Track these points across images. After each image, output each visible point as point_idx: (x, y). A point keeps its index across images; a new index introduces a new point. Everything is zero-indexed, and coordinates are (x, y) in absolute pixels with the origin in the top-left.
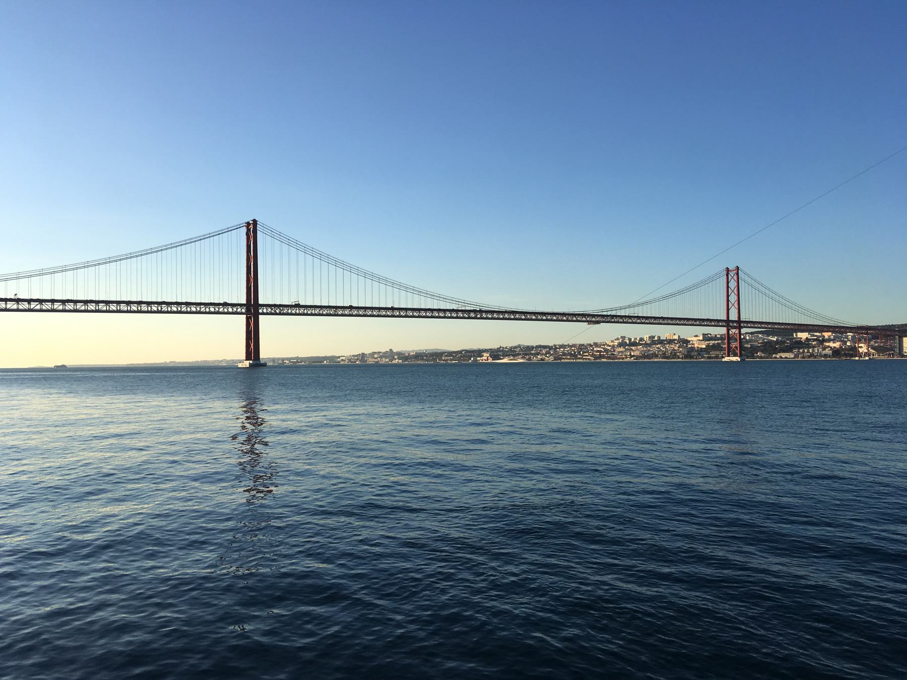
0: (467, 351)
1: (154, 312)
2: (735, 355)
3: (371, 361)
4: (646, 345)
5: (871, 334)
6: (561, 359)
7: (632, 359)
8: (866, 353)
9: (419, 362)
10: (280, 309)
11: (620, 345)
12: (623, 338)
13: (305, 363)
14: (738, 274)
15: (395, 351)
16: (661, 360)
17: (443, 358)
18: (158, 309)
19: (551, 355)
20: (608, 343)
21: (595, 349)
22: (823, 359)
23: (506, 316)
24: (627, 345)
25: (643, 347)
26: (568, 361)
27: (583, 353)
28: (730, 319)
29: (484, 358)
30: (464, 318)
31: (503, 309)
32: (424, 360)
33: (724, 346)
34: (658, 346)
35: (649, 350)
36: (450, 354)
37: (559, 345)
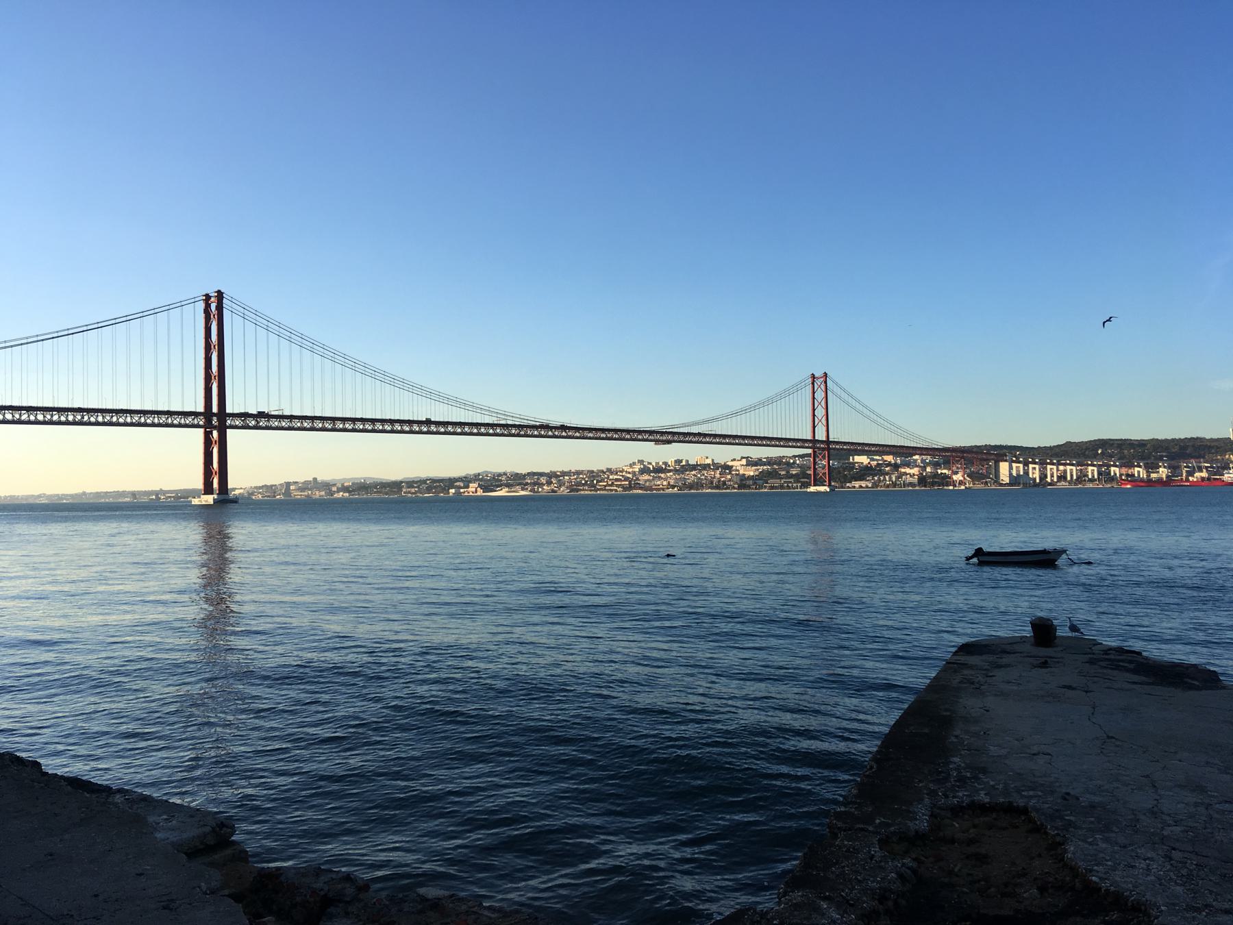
3: (298, 495)
4: (676, 471)
6: (578, 490)
7: (676, 489)
10: (256, 420)
11: (642, 471)
12: (641, 462)
14: (826, 382)
15: (319, 479)
20: (625, 468)
21: (611, 477)
22: (911, 488)
24: (652, 472)
26: (589, 492)
27: (598, 482)
28: (816, 438)
29: (470, 489)
33: (808, 472)
34: (693, 472)
36: (410, 484)
37: (560, 472)
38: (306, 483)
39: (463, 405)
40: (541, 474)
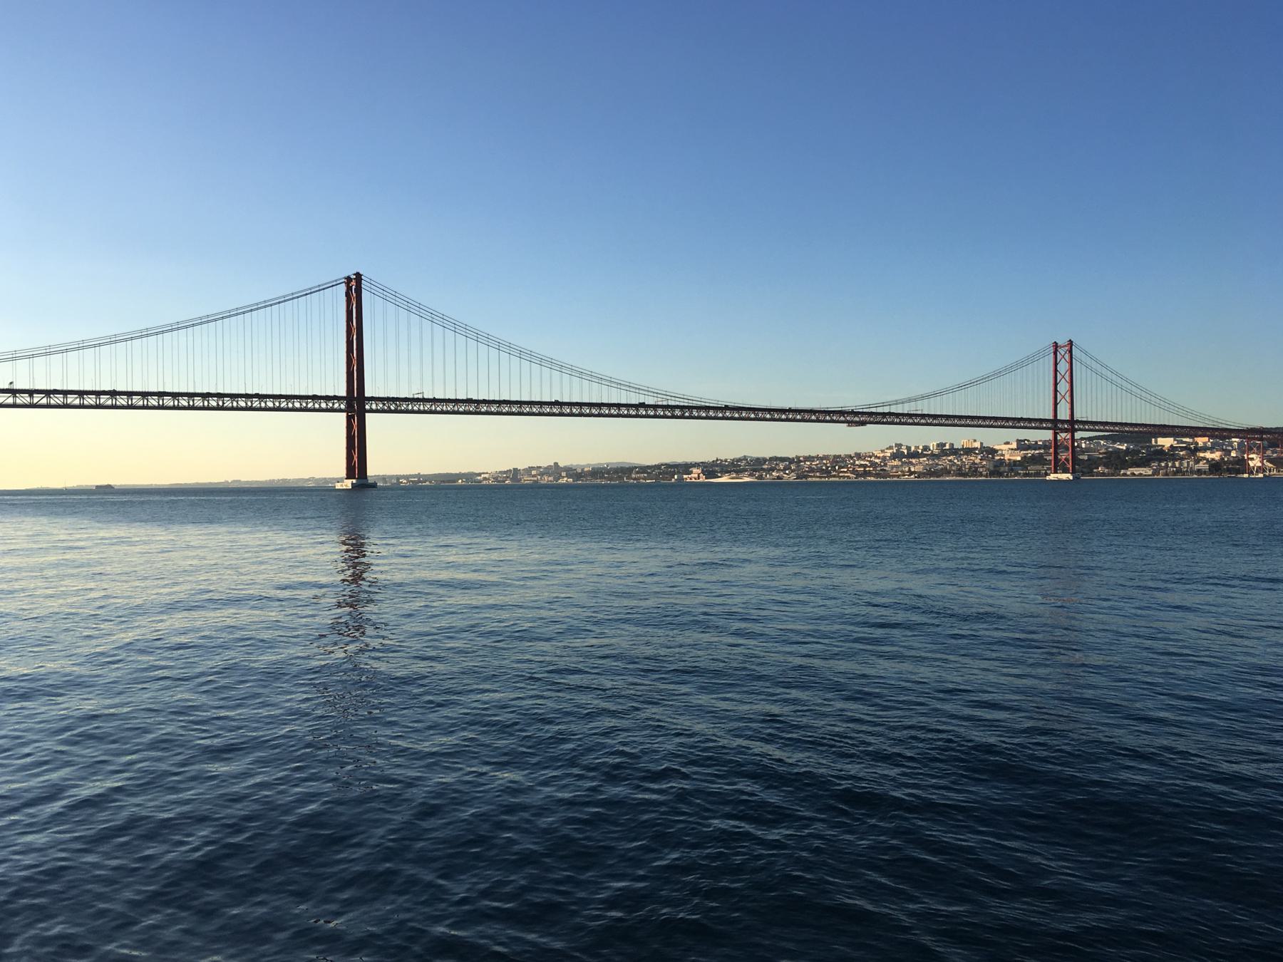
0: (668, 466)
1: (184, 408)
2: (1065, 471)
3: (527, 480)
4: (933, 456)
5: (1267, 439)
6: (806, 477)
8: (1259, 467)
9: (598, 481)
11: (894, 457)
12: (899, 446)
13: (430, 482)
14: (1071, 351)
15: (561, 465)
16: (954, 478)
17: (633, 476)
18: (218, 404)
19: (793, 471)
20: (876, 453)
21: (857, 463)
22: (1195, 476)
23: (727, 414)
24: (905, 457)
25: (928, 460)
26: (818, 479)
28: (1058, 418)
29: (693, 475)
30: (665, 417)
31: (722, 404)
32: (605, 478)
33: (1048, 458)
35: (937, 464)
36: (643, 469)
37: (805, 457)
38: (549, 468)
39: (620, 385)
40: (783, 459)
